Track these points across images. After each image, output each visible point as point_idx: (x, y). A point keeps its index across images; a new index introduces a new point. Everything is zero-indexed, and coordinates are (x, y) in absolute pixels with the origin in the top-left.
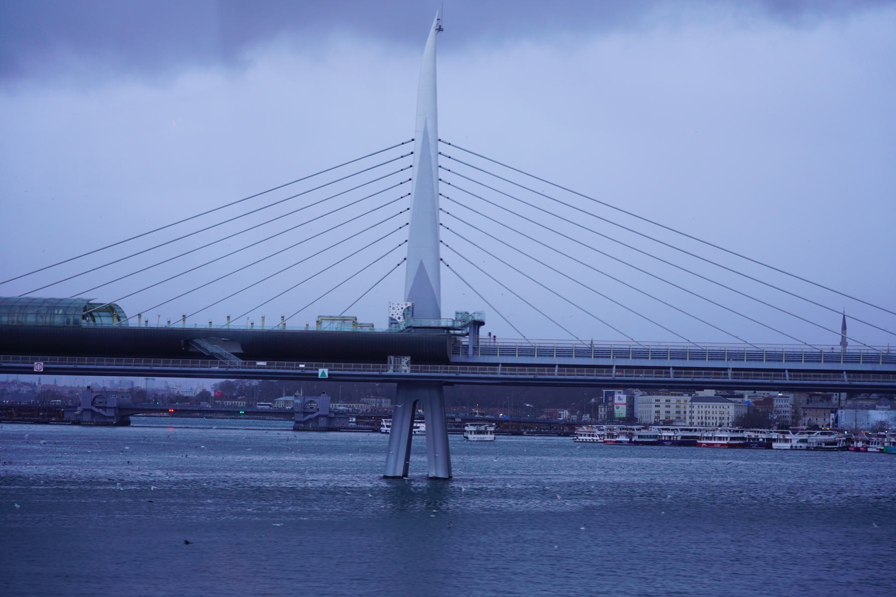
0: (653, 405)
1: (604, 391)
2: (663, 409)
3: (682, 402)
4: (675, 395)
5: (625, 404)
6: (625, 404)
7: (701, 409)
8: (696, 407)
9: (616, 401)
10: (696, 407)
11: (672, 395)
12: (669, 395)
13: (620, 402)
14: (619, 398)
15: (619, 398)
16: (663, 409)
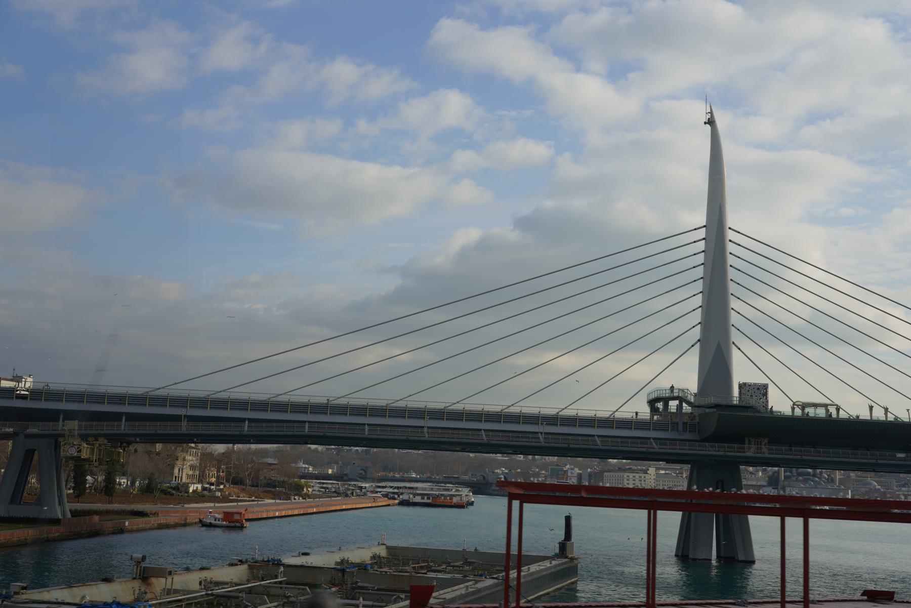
0: (626, 480)
1: (550, 467)
2: (631, 482)
3: (643, 477)
4: (638, 473)
5: (575, 477)
6: (575, 477)
7: (664, 483)
8: (661, 481)
9: (569, 474)
10: (661, 481)
11: (636, 473)
12: (634, 473)
13: (571, 475)
14: (572, 473)
15: (572, 473)
16: (631, 482)
